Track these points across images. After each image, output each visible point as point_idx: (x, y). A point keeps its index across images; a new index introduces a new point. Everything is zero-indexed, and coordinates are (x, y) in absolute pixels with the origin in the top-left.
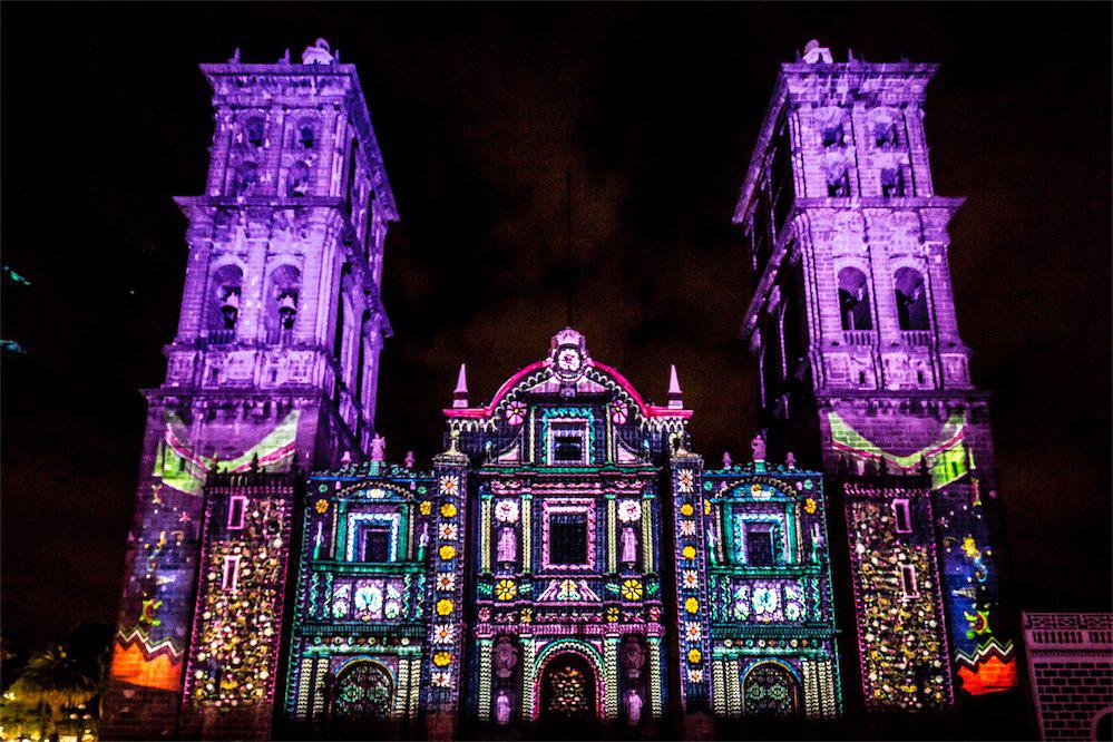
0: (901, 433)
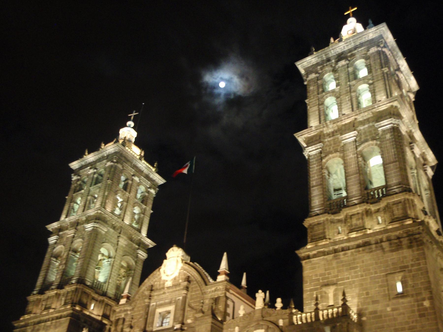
0: (356, 267)
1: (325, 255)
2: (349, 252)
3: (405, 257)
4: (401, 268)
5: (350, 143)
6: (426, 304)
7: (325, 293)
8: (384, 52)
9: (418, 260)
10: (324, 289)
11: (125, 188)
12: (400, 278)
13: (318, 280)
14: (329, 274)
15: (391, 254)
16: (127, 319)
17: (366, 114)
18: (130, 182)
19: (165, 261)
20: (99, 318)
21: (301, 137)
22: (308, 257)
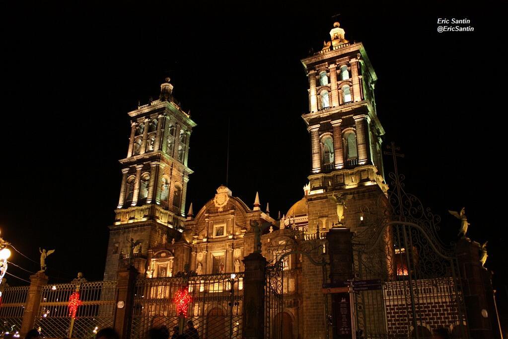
1: (321, 199)
5: (337, 127)
8: (360, 63)
10: (320, 219)
11: (172, 133)
13: (317, 214)
16: (193, 229)
17: (348, 108)
18: (175, 129)
19: (216, 195)
20: (166, 225)
21: (306, 118)
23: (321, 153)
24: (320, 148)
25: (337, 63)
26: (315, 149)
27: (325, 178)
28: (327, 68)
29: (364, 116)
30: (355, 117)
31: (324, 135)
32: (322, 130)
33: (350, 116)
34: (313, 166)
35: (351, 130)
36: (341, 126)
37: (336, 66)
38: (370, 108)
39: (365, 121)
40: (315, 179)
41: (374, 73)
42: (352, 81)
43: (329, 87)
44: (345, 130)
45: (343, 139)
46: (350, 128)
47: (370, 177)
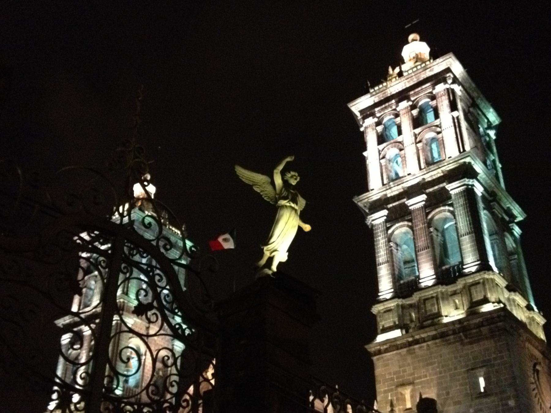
0: (434, 363)
1: (398, 349)
2: (424, 344)
3: (487, 349)
4: (484, 361)
5: (418, 209)
6: (512, 403)
7: (402, 394)
8: (453, 90)
9: (501, 352)
10: (400, 390)
12: (482, 373)
13: (392, 379)
14: (404, 371)
15: (469, 346)
17: (435, 172)
22: (379, 352)
23: (393, 262)
24: (390, 253)
25: (412, 99)
26: (382, 255)
27: (403, 307)
28: (395, 110)
29: (471, 182)
30: (449, 187)
31: (397, 228)
32: (391, 220)
33: (441, 185)
34: (380, 288)
35: (444, 211)
36: (425, 207)
37: (410, 103)
38: (478, 167)
39: (469, 193)
40: (385, 312)
41: (491, 110)
42: (440, 124)
43: (400, 142)
44: (433, 213)
45: (432, 229)
46: (442, 208)
47: (489, 295)
